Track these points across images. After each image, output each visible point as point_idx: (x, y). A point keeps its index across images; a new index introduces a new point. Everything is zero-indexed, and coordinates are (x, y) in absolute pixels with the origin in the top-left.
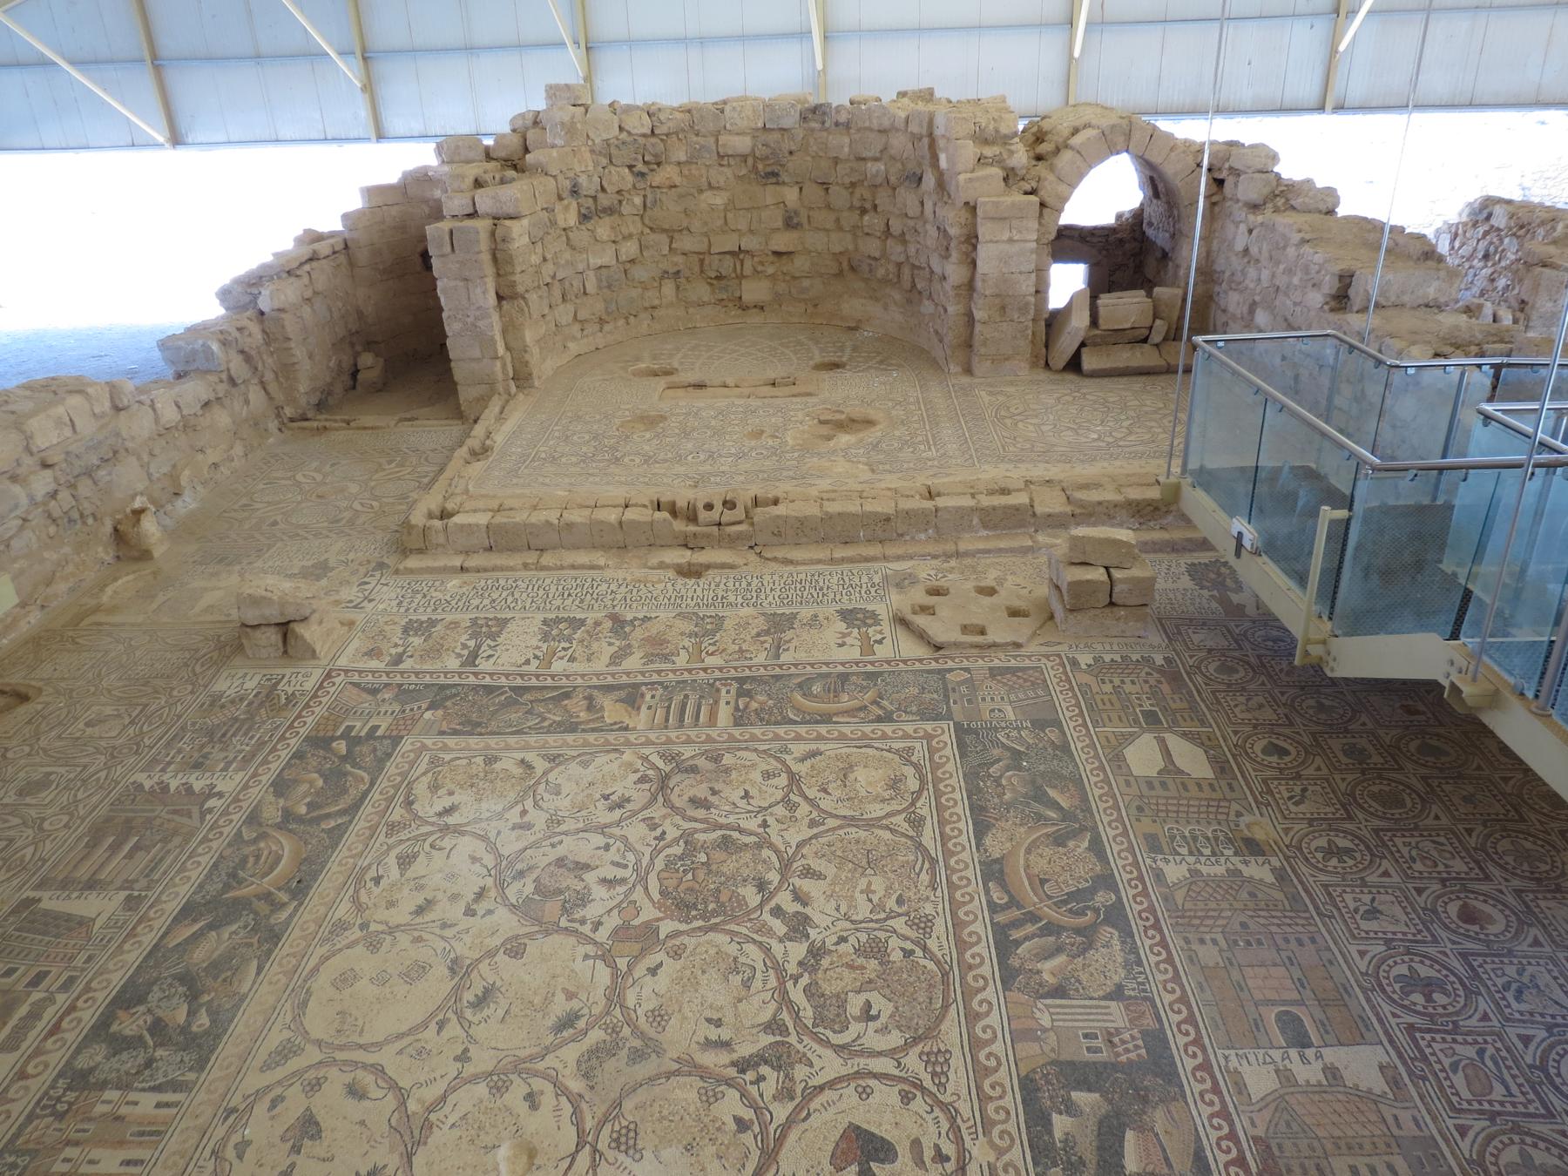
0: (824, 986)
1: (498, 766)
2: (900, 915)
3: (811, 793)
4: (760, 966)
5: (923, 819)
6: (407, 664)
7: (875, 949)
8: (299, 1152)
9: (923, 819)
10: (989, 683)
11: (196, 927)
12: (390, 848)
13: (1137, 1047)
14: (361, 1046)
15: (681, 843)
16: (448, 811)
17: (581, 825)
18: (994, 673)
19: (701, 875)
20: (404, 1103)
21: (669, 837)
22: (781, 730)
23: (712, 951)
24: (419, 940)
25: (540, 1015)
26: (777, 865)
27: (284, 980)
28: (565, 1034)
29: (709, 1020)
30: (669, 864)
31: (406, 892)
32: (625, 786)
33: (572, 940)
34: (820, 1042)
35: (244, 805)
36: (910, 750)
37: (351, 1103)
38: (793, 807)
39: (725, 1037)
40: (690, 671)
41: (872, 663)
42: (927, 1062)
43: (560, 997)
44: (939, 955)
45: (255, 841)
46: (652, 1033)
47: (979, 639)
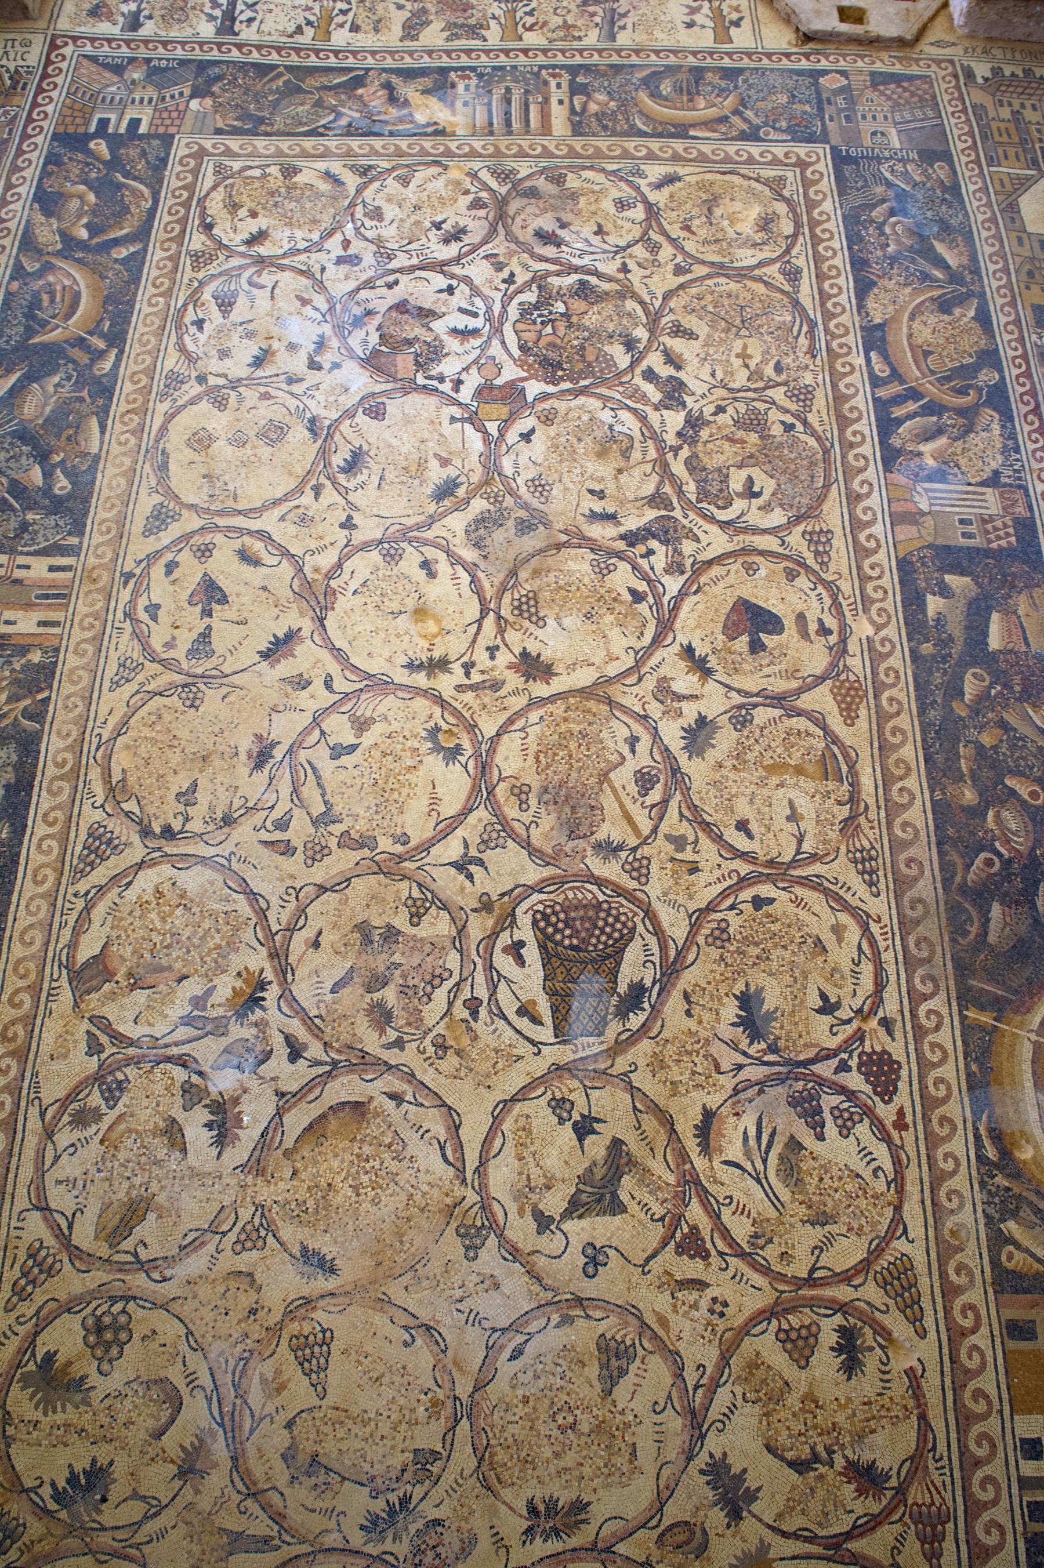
0: (706, 460)
1: (298, 179)
2: (779, 384)
3: (675, 232)
4: (637, 435)
5: (799, 271)
6: (148, 29)
7: (755, 422)
8: (210, 616)
9: (799, 271)
10: (869, 94)
11: (13, 379)
12: (201, 283)
13: (1008, 534)
14: (240, 512)
15: (534, 287)
16: (258, 238)
17: (415, 261)
18: (878, 80)
19: (561, 332)
20: (301, 570)
21: (520, 280)
22: (630, 144)
23: (585, 418)
24: (266, 396)
25: (417, 482)
26: (644, 320)
27: (133, 441)
28: (446, 502)
29: (591, 492)
30: (525, 311)
31: (235, 338)
32: (456, 212)
33: (433, 401)
34: (704, 517)
35: (12, 225)
36: (782, 179)
37: (247, 570)
38: (654, 248)
39: (610, 510)
40: (507, 52)
41: (730, 55)
42: (810, 541)
43: (434, 464)
44: (819, 429)
45: (40, 274)
46: (535, 503)
47: (857, 29)
